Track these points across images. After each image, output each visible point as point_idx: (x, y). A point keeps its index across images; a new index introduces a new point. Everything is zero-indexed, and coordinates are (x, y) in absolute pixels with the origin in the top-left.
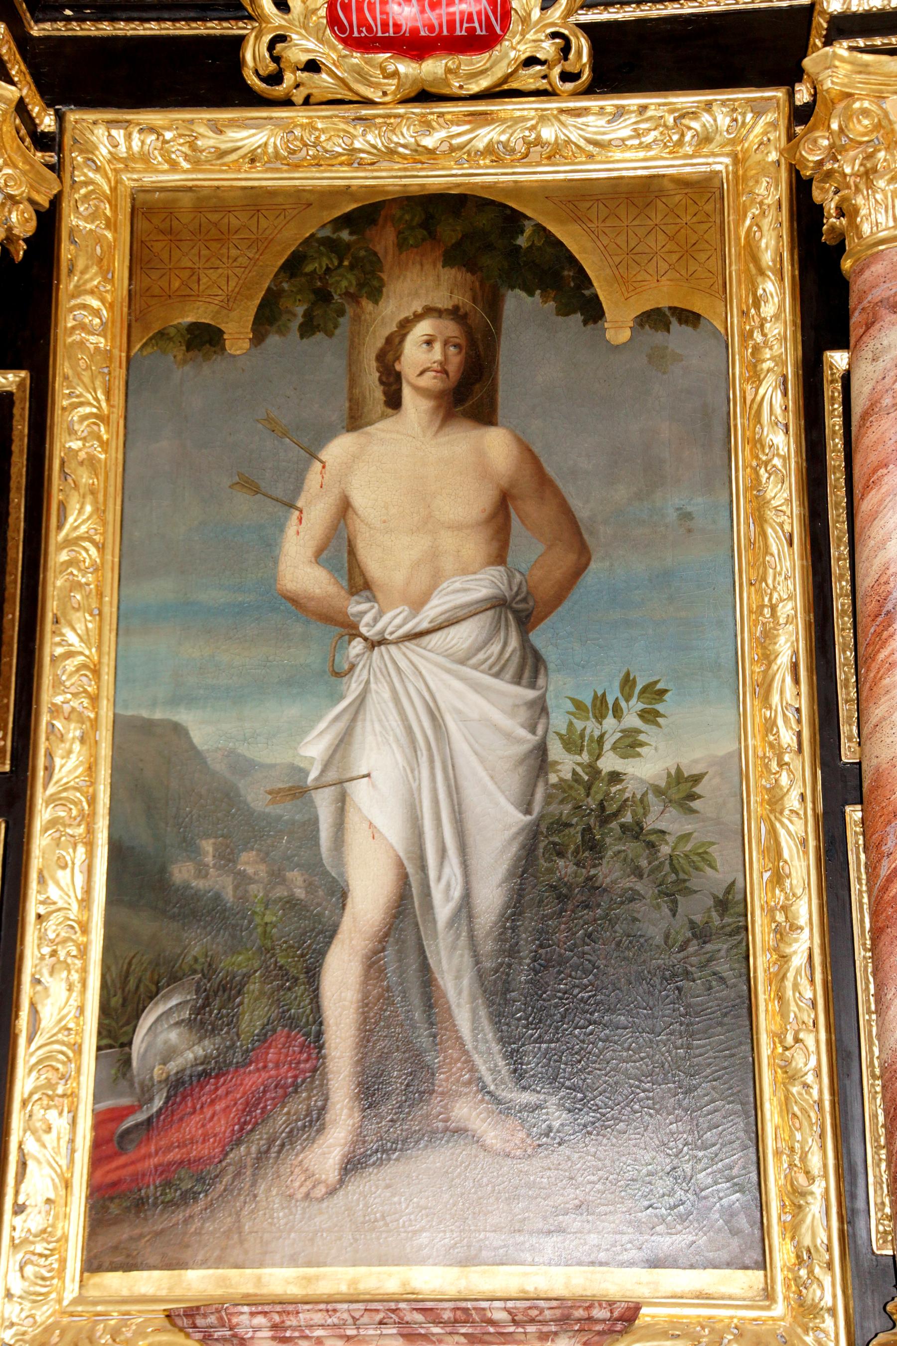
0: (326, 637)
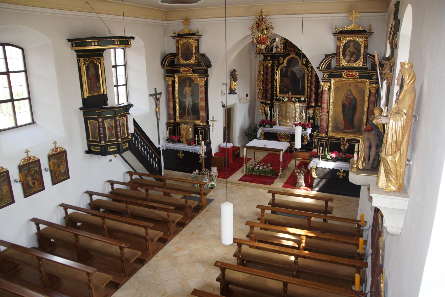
0: (185, 96)
